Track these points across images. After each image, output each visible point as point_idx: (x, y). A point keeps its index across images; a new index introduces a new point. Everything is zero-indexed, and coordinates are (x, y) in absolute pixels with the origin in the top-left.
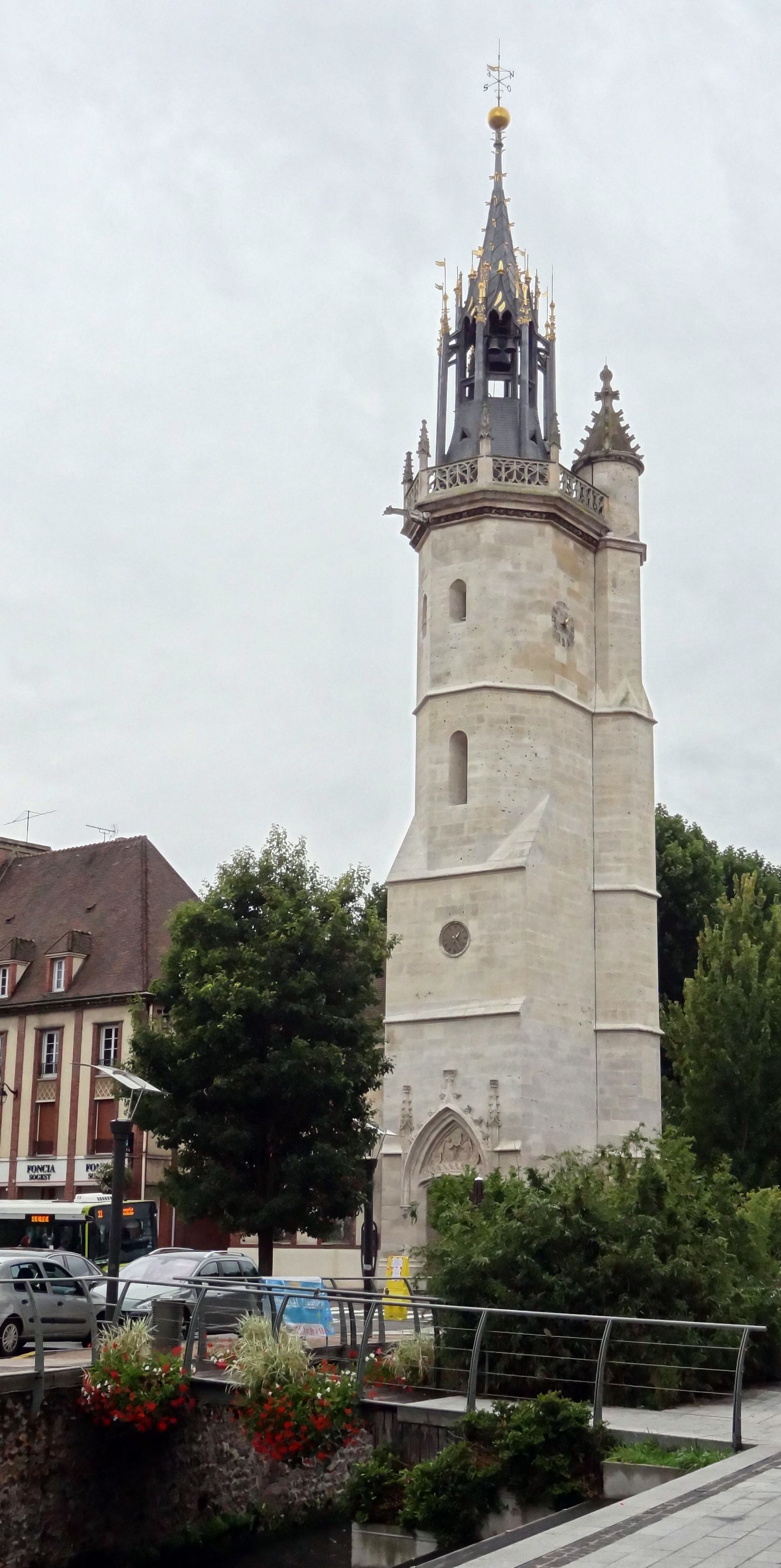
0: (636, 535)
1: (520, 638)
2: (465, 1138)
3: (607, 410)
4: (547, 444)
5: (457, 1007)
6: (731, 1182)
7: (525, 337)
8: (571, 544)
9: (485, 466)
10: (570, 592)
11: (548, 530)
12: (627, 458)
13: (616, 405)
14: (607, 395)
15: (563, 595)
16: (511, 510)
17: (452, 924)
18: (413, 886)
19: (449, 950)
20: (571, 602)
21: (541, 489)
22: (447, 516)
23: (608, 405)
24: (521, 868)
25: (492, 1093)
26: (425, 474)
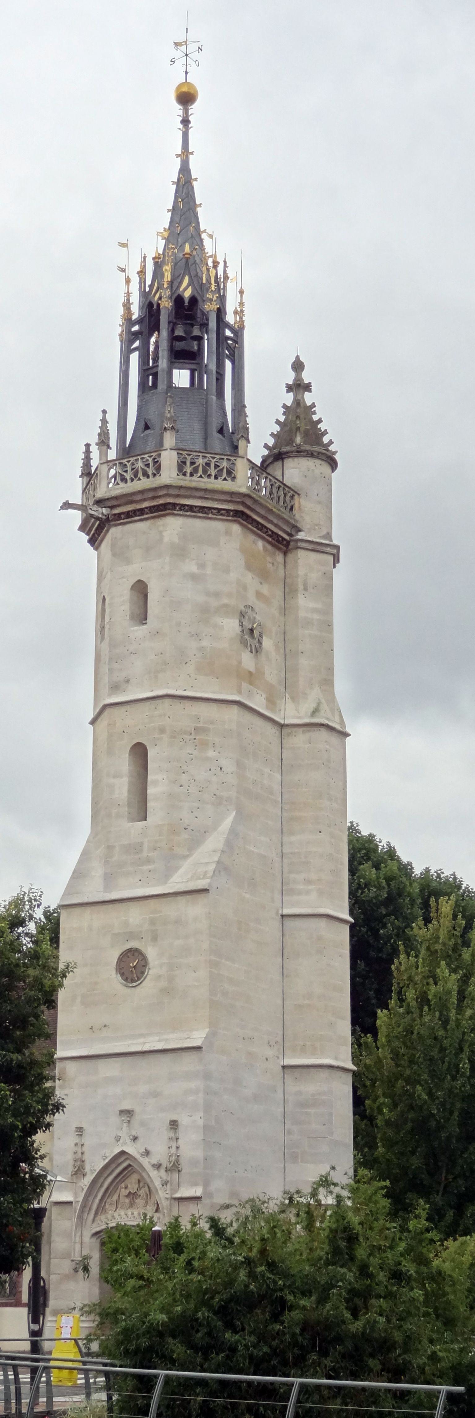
0: (328, 536)
1: (205, 643)
2: (141, 1184)
3: (298, 403)
4: (234, 437)
5: (135, 1042)
6: (428, 1230)
7: (213, 324)
8: (260, 543)
9: (169, 459)
10: (259, 595)
11: (236, 528)
12: (319, 453)
13: (308, 398)
14: (299, 387)
15: (252, 599)
16: (196, 507)
17: (130, 950)
18: (89, 910)
19: (126, 980)
20: (258, 605)
21: (228, 485)
22: (128, 512)
23: (299, 397)
24: (205, 891)
25: (172, 1134)
26: (105, 468)
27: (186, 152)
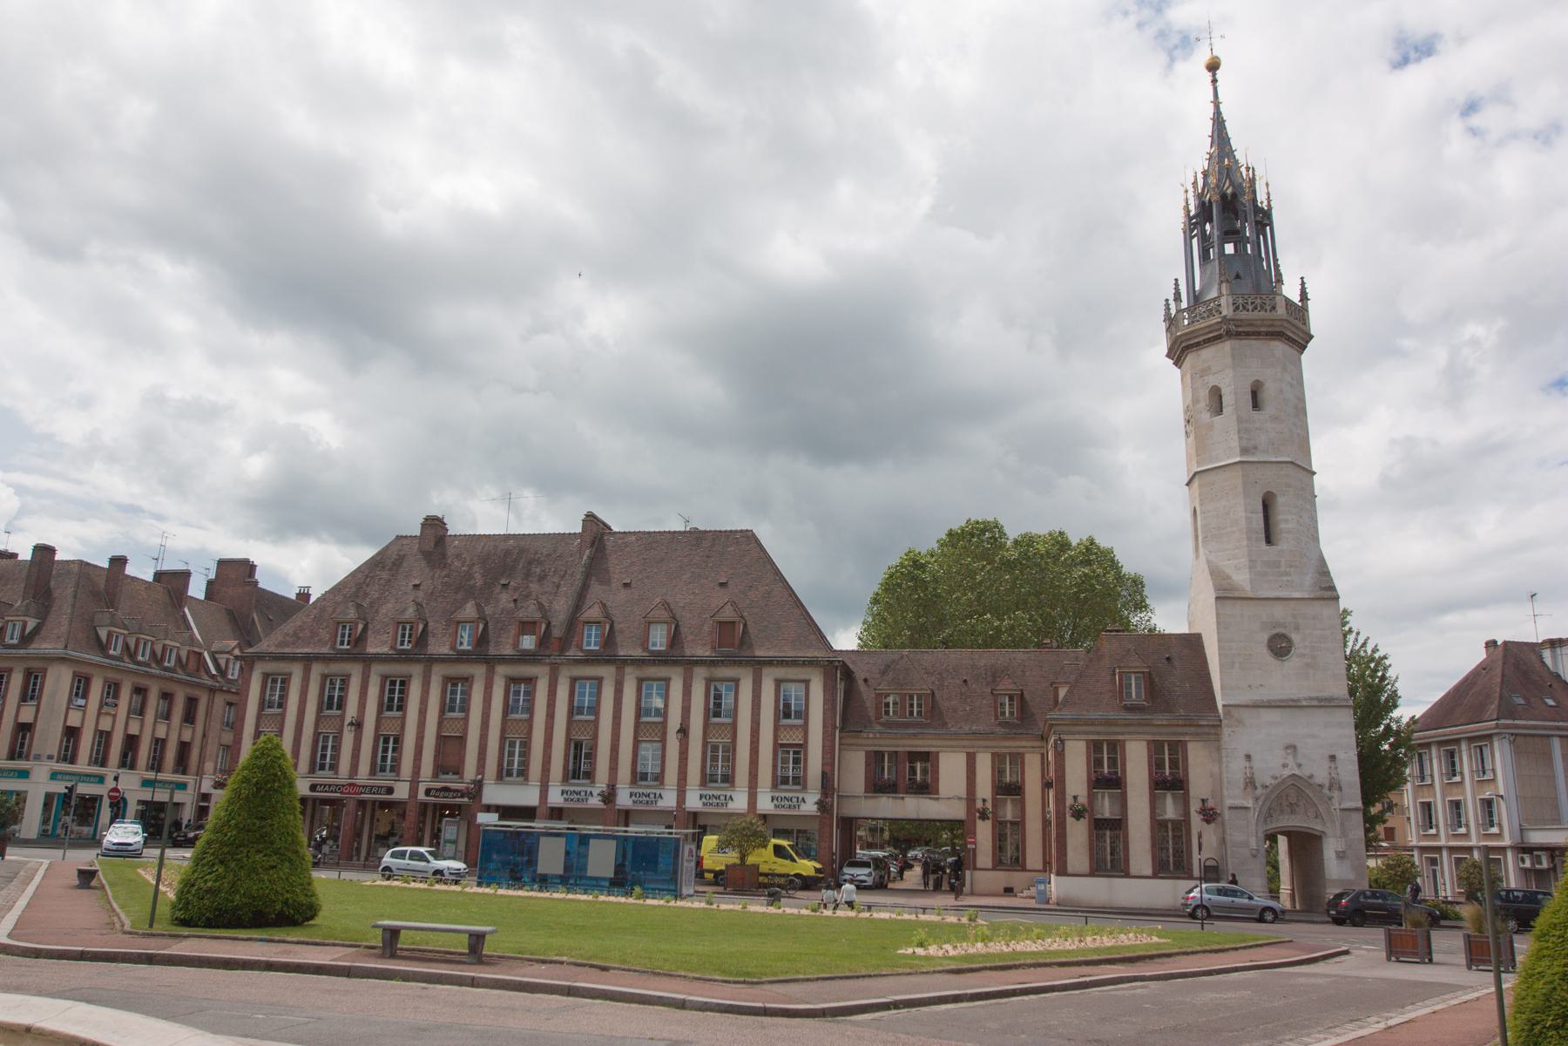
27: (1216, 103)
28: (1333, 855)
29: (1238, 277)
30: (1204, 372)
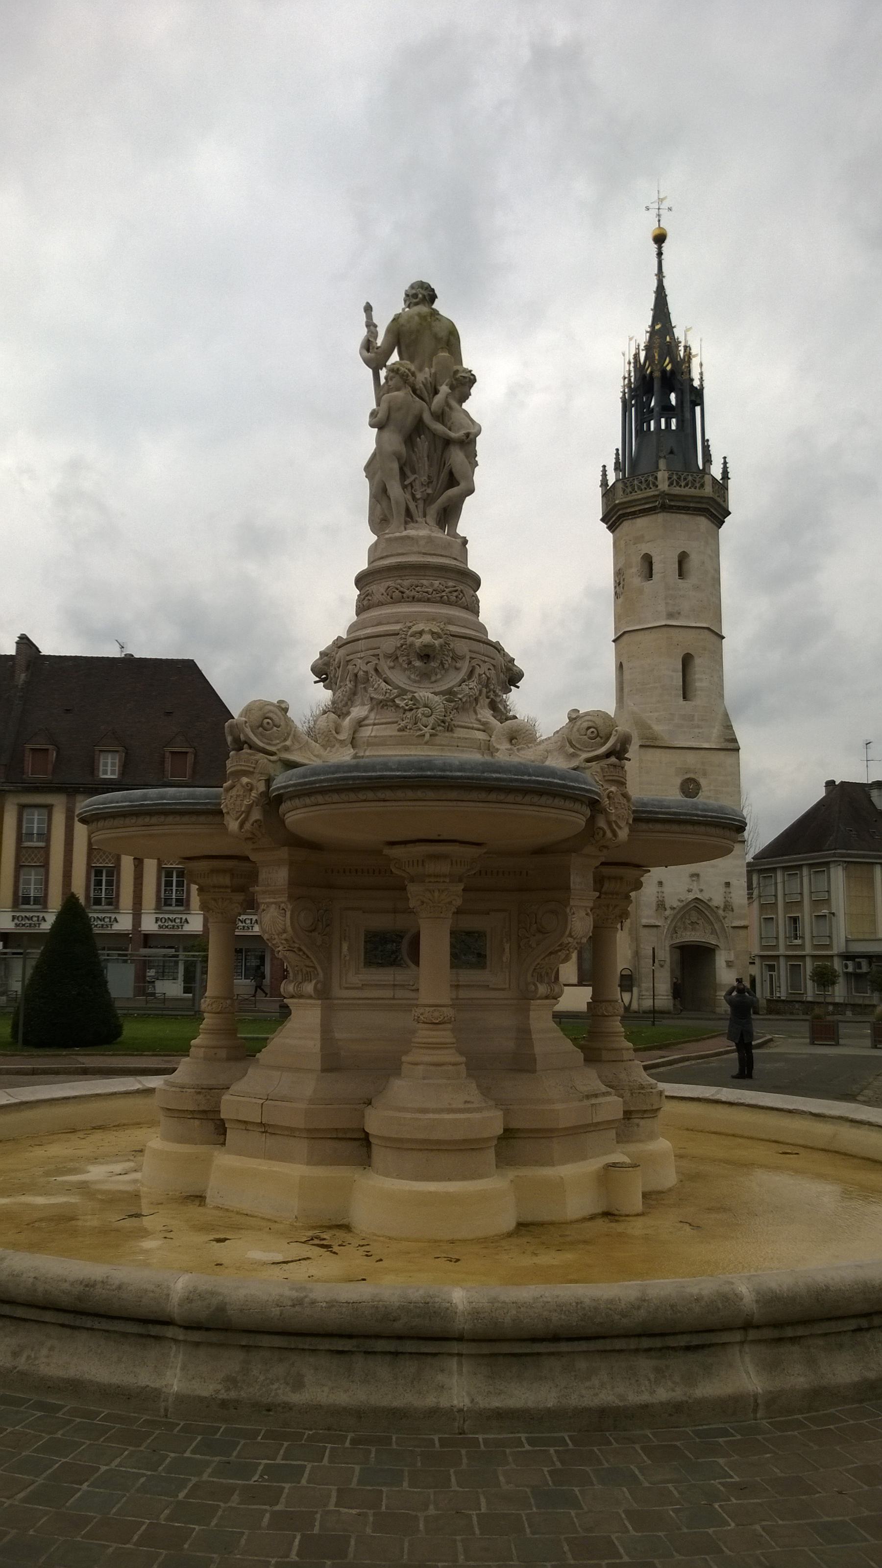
28: (724, 964)
29: (672, 452)
30: (639, 539)
